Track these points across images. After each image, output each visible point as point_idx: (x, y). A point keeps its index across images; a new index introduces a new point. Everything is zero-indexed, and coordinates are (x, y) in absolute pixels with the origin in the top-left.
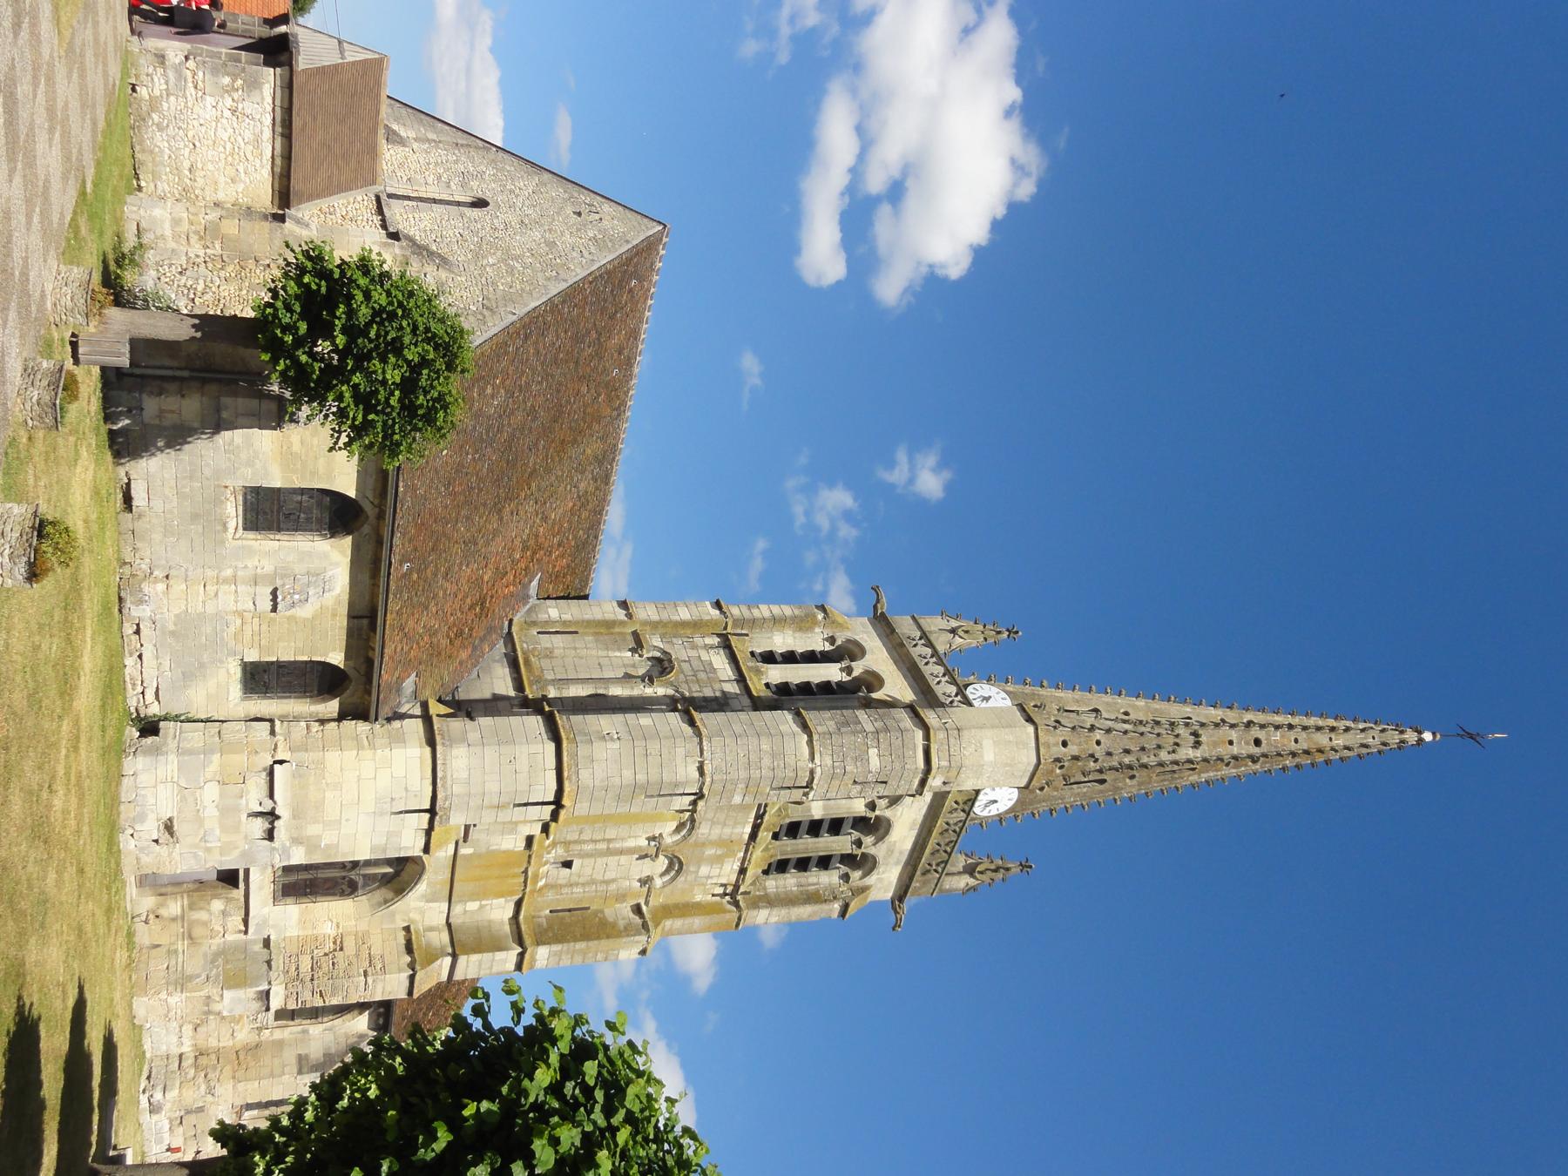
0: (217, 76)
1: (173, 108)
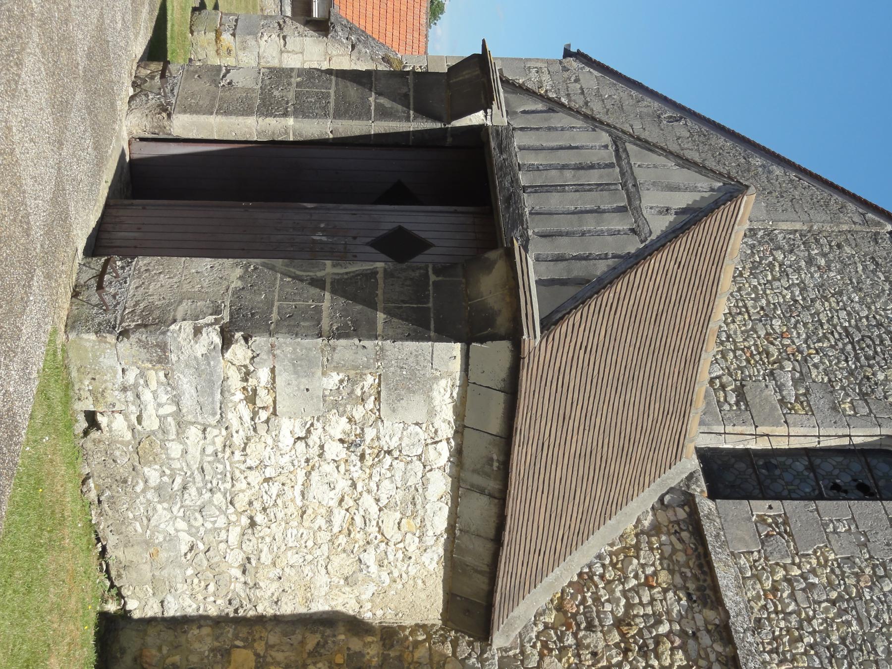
0: (310, 375)
1: (194, 452)
